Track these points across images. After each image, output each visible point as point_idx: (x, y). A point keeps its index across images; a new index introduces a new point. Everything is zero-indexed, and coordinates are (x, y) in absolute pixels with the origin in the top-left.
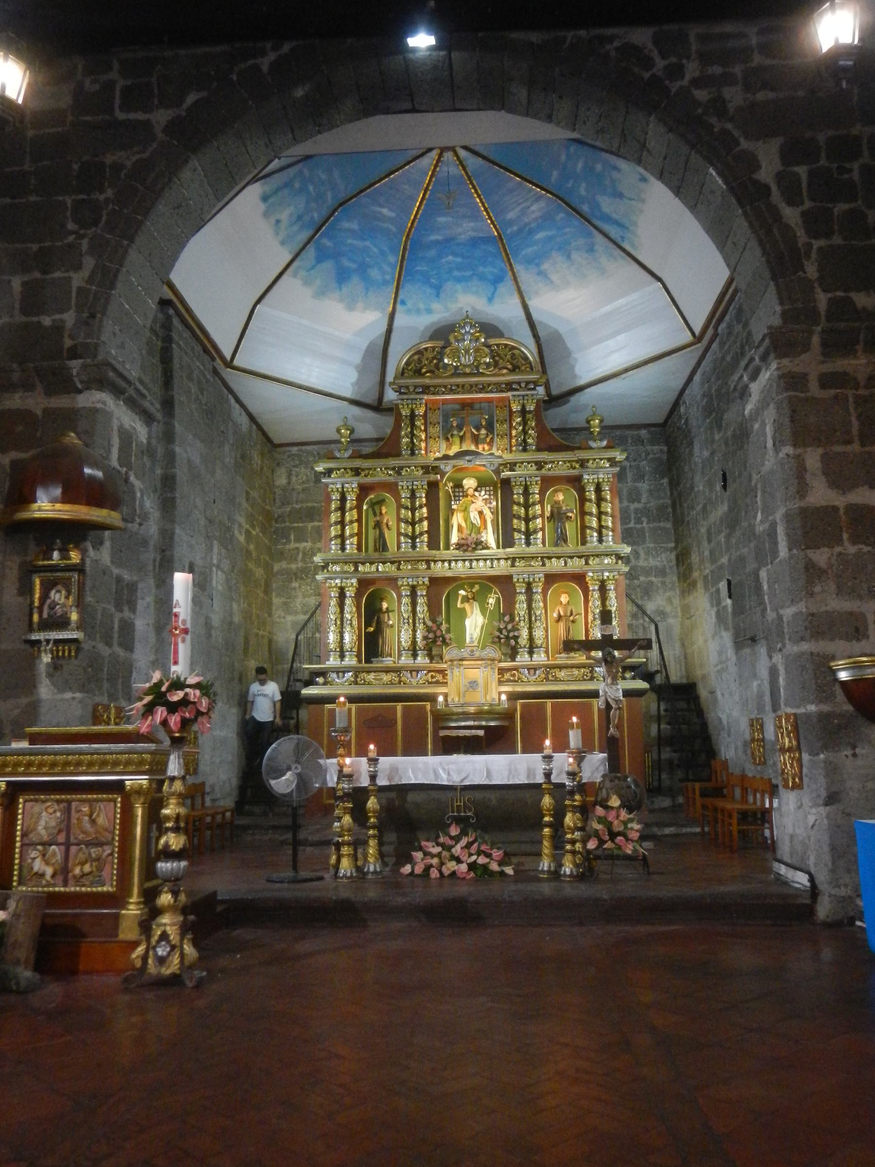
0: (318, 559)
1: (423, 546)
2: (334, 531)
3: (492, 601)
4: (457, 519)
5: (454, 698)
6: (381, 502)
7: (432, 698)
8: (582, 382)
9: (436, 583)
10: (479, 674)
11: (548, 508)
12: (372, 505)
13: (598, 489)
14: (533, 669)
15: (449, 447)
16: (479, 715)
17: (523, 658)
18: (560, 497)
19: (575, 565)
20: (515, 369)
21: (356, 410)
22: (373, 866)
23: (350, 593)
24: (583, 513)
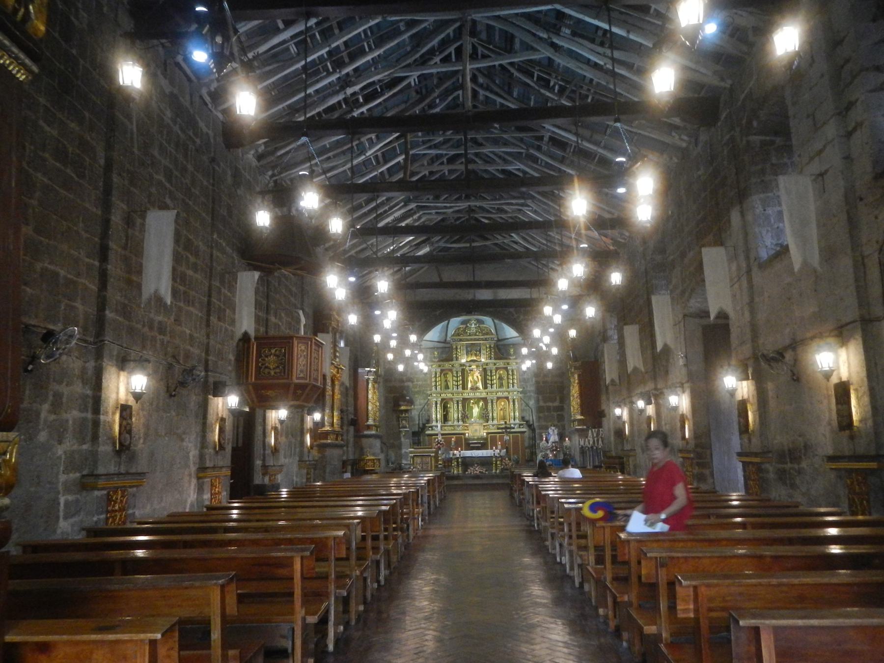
0: (429, 392)
1: (460, 389)
2: (433, 384)
3: (481, 404)
4: (470, 378)
5: (471, 434)
6: (447, 374)
7: (464, 434)
8: (508, 337)
9: (465, 400)
10: (477, 427)
11: (498, 376)
12: (444, 375)
13: (512, 371)
14: (493, 425)
15: (467, 358)
16: (478, 439)
17: (490, 422)
18: (501, 372)
19: (506, 394)
20: (487, 334)
21: (436, 344)
22: (460, 472)
23: (439, 403)
24: (508, 378)
